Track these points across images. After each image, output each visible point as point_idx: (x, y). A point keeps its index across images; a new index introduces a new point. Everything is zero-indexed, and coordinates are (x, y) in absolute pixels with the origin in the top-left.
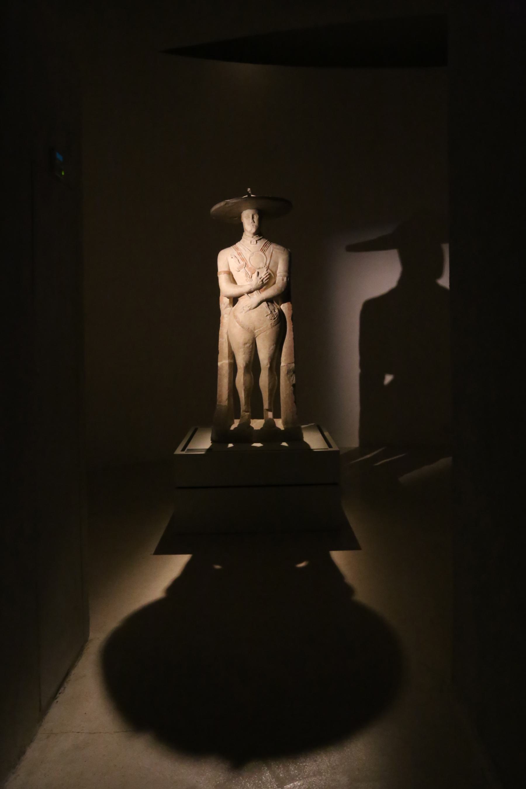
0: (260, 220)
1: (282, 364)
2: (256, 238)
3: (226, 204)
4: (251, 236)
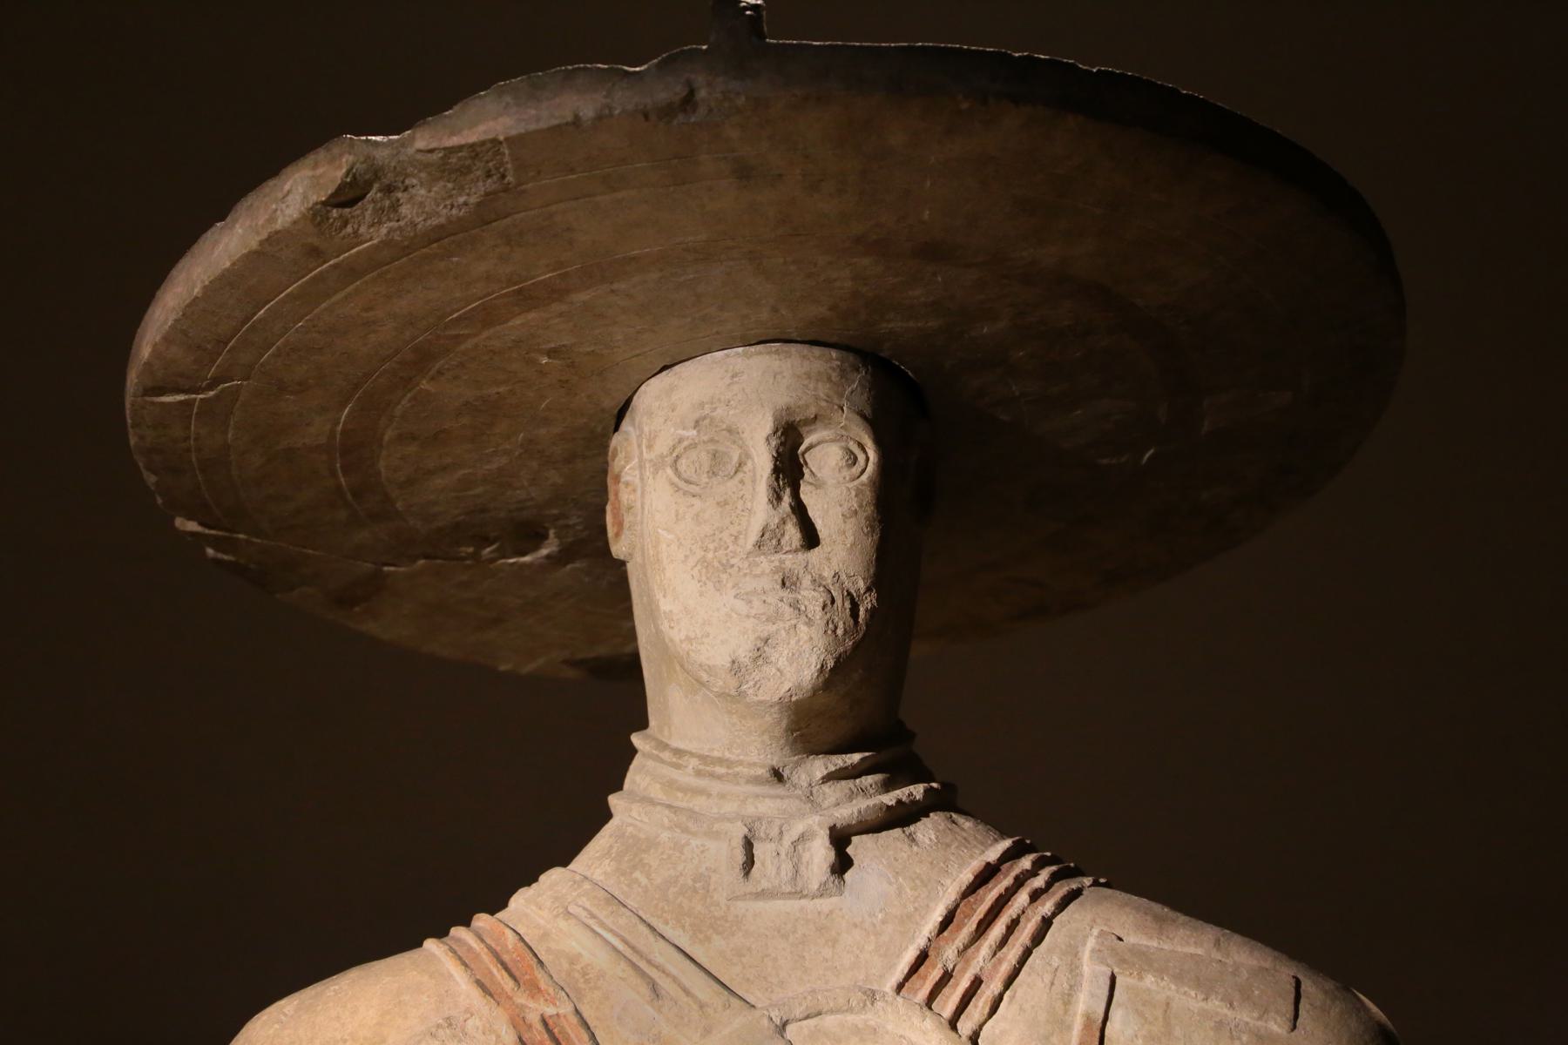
0: (897, 509)
2: (830, 795)
3: (348, 196)
4: (759, 746)
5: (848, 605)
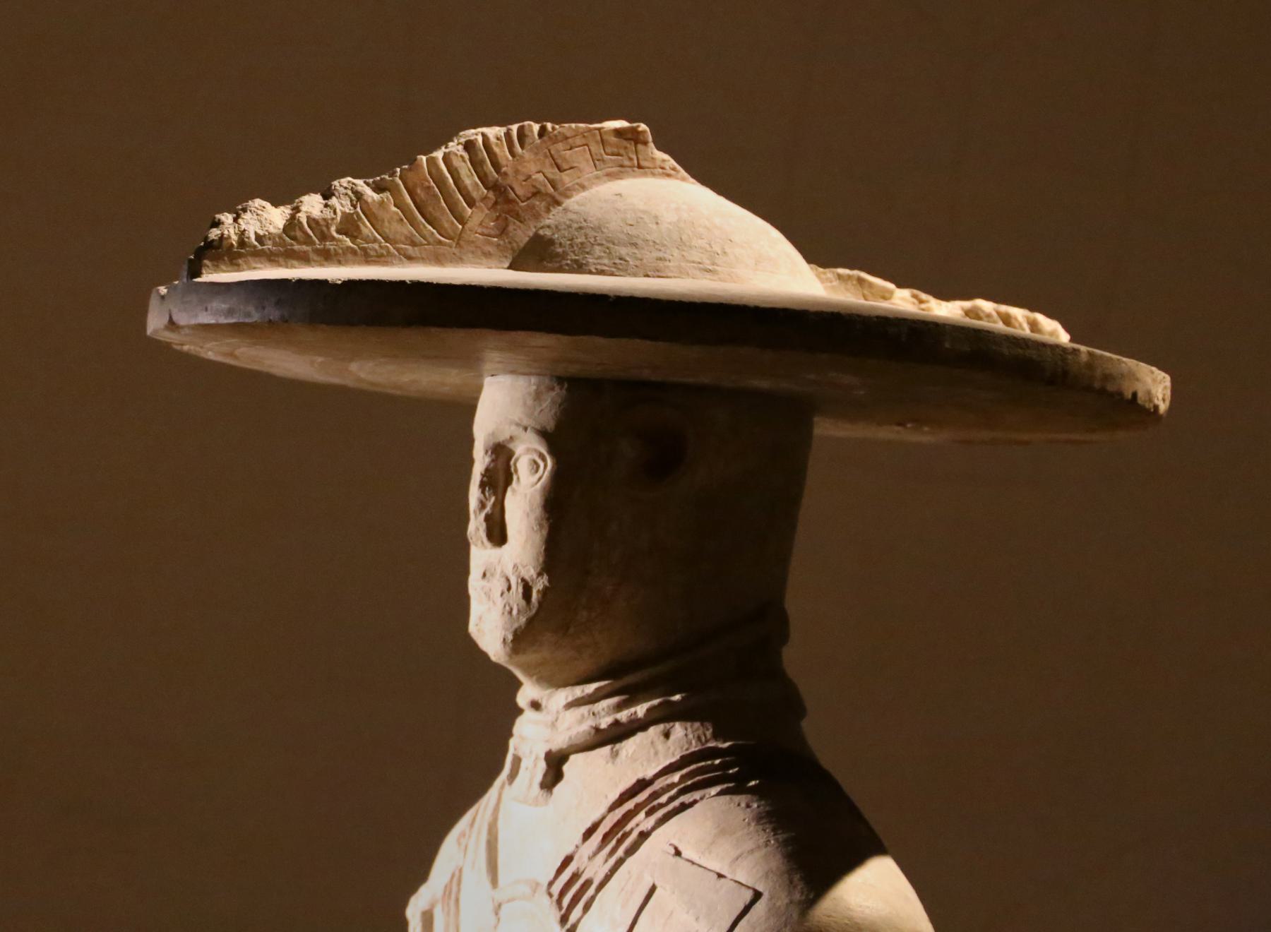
5: (521, 590)
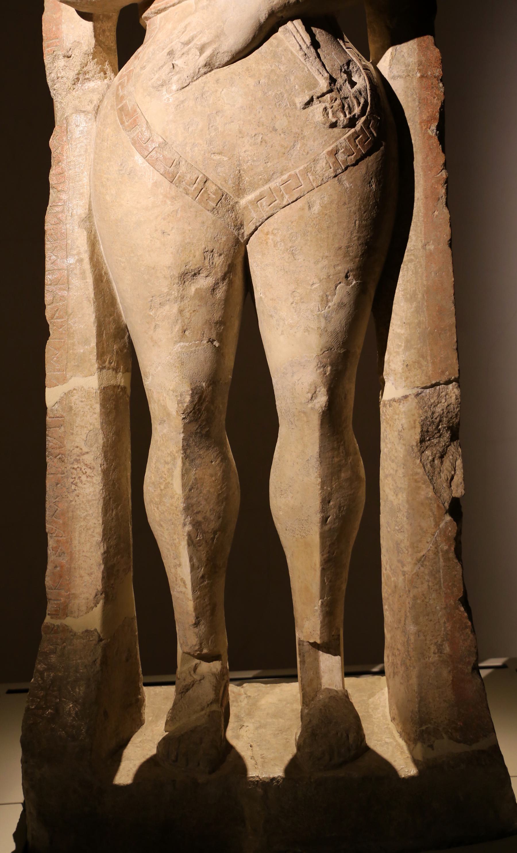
1: (392, 390)
